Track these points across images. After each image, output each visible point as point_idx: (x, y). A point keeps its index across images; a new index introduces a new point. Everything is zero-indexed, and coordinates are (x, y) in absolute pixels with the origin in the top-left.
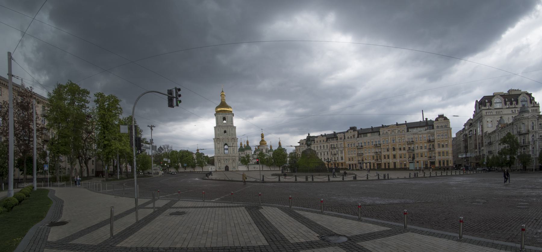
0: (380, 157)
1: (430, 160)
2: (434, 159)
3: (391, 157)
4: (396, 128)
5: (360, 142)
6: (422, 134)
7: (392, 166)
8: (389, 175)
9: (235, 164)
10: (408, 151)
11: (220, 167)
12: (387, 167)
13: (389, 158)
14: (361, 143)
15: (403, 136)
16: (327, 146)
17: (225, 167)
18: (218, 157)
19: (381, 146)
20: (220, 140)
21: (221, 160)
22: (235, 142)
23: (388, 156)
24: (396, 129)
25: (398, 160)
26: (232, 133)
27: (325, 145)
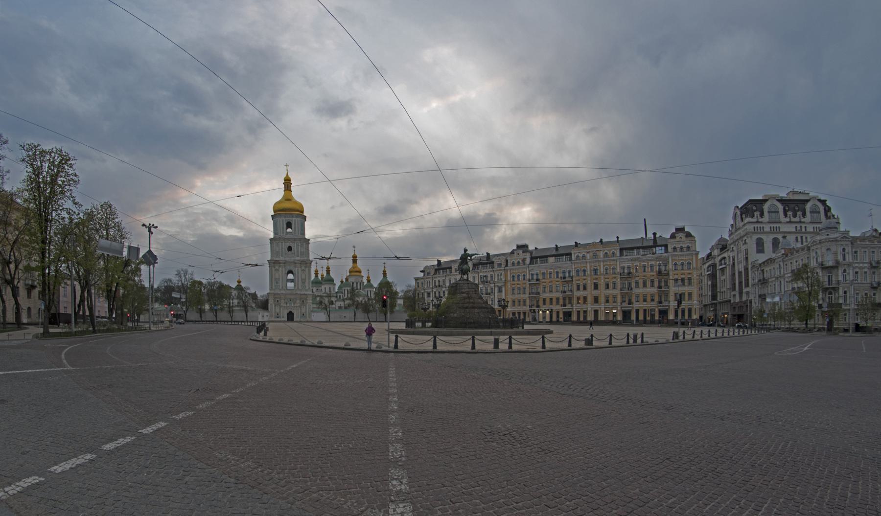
0: (570, 299)
2: (666, 306)
3: (590, 299)
4: (602, 249)
5: (535, 272)
6: (648, 260)
7: (590, 317)
9: (306, 309)
10: (621, 290)
11: (278, 314)
12: (582, 319)
14: (537, 274)
15: (613, 262)
17: (288, 314)
18: (276, 296)
20: (280, 263)
22: (306, 267)
23: (585, 298)
24: (601, 250)
26: (302, 250)
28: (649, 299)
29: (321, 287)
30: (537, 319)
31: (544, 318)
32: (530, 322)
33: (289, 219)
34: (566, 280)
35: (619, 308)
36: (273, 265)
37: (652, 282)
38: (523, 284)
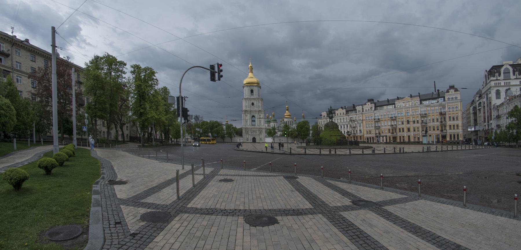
0: (395, 130)
1: (442, 134)
3: (405, 130)
7: (406, 140)
8: (404, 148)
9: (262, 136)
12: (402, 141)
13: (403, 131)
15: (417, 108)
16: (347, 119)
18: (247, 129)
19: (396, 119)
20: (248, 112)
21: (249, 131)
23: (403, 129)
25: (412, 134)
26: (259, 105)
27: (345, 117)
28: (436, 129)
29: (270, 124)
30: (379, 141)
31: (383, 140)
32: (376, 143)
33: (252, 88)
34: (393, 119)
35: (421, 134)
36: (244, 113)
37: (437, 119)
38: (369, 122)
